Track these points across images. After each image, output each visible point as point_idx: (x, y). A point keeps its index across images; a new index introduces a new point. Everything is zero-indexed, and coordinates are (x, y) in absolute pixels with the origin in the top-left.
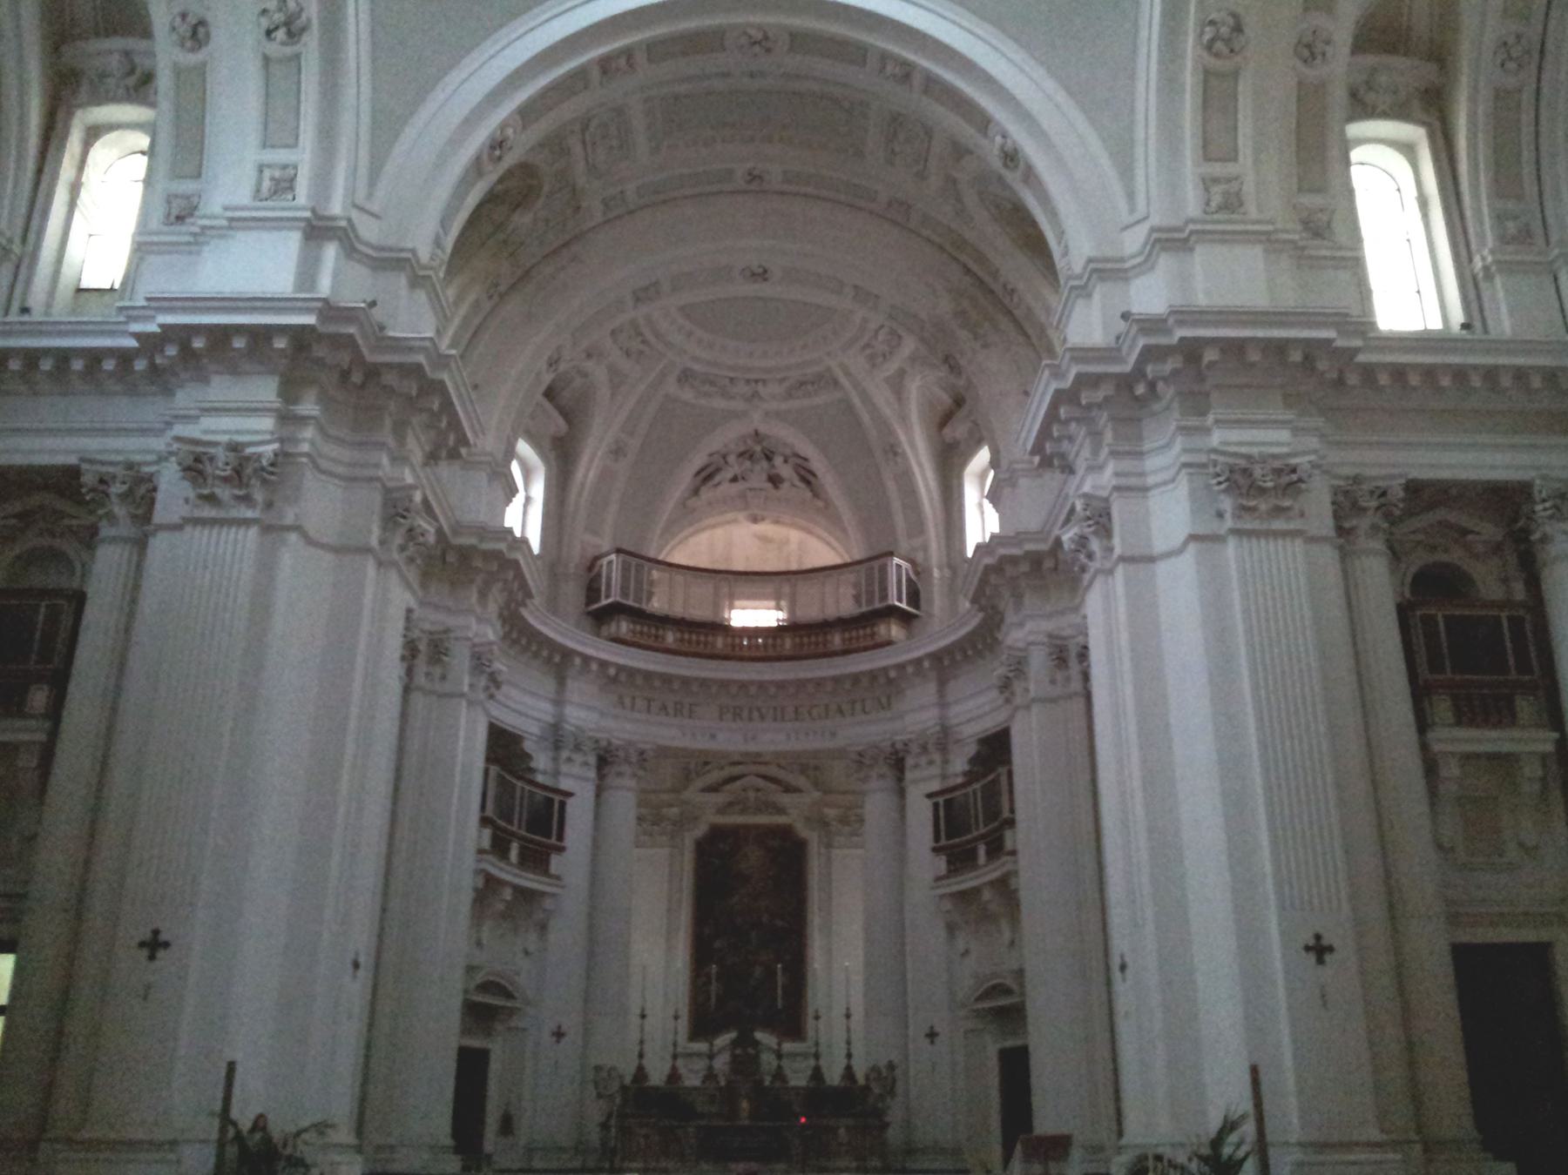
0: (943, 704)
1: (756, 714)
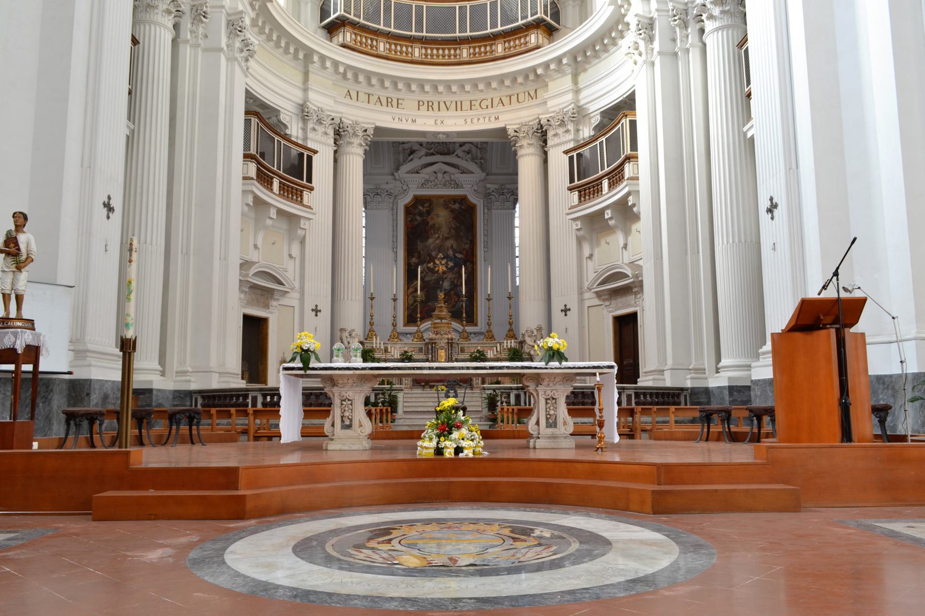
0: (577, 91)
1: (442, 105)
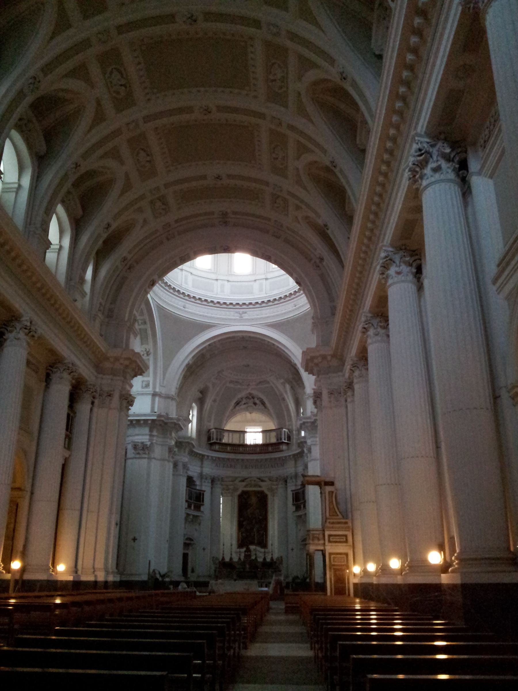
0: (296, 467)
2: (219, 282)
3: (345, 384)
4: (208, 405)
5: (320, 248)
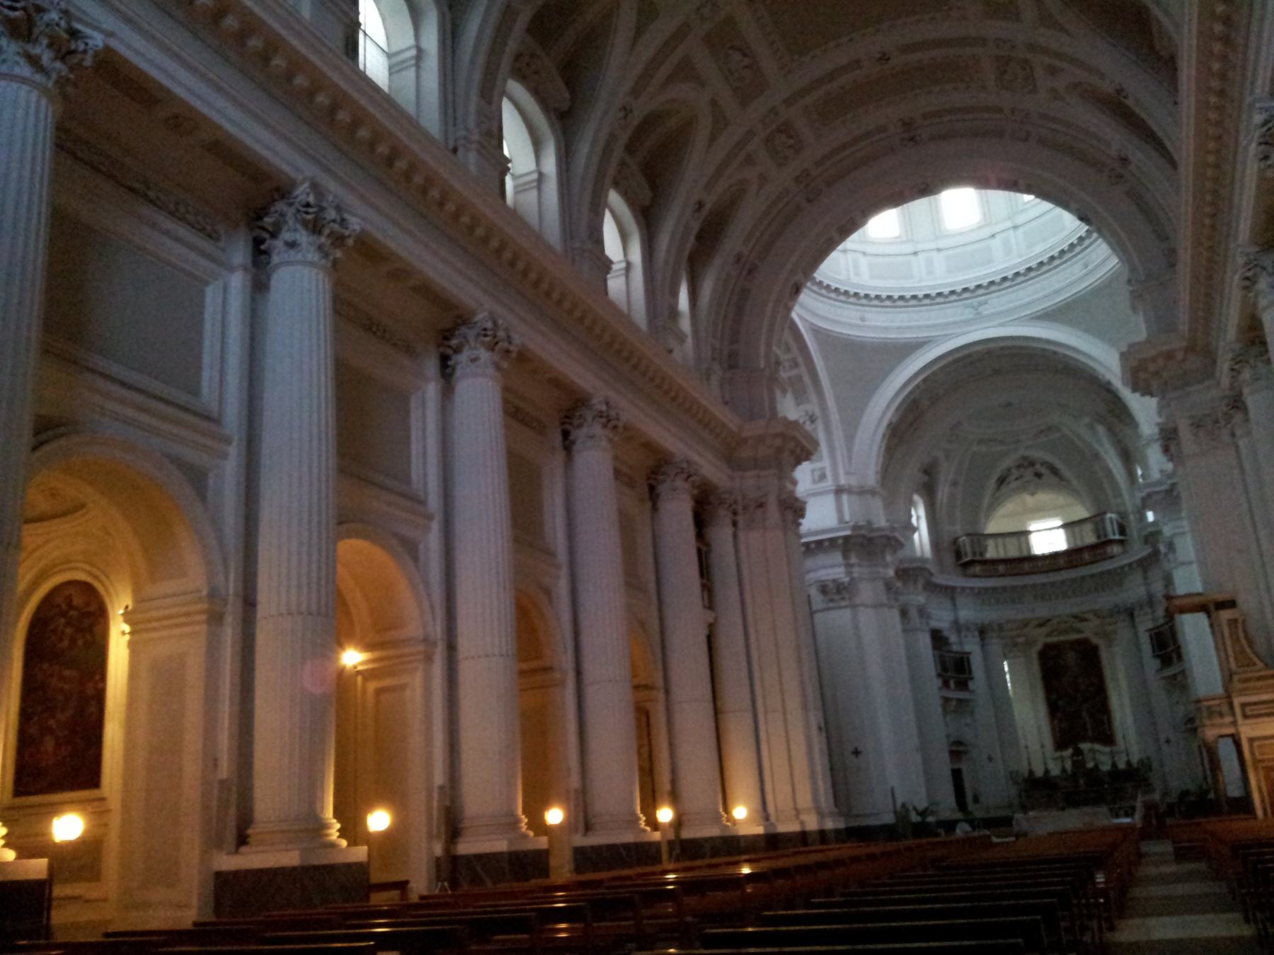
2: (920, 256)
3: (1225, 401)
4: (942, 494)
5: (1115, 138)
